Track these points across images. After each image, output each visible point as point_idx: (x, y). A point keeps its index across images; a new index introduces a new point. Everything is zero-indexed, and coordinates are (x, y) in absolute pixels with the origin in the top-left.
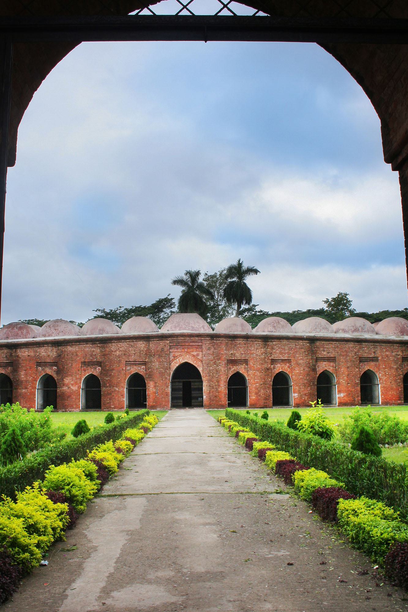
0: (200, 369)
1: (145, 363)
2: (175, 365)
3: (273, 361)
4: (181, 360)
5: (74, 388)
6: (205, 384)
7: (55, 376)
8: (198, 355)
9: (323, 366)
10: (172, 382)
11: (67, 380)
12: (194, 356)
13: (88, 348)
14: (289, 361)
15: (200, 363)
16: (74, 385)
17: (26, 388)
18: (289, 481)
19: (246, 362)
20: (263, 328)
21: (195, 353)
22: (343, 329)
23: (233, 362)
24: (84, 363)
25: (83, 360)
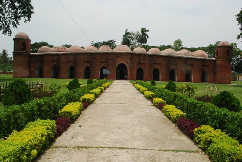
0: (127, 66)
1: (106, 62)
2: (118, 64)
3: (154, 64)
4: (120, 62)
5: (81, 71)
6: (128, 71)
7: (73, 66)
8: (126, 60)
9: (172, 67)
10: (116, 70)
12: (124, 61)
13: (86, 57)
14: (160, 64)
15: (127, 64)
16: (81, 70)
18: (191, 136)
19: (144, 64)
21: (125, 60)
22: (181, 53)
23: (139, 63)
24: (84, 62)
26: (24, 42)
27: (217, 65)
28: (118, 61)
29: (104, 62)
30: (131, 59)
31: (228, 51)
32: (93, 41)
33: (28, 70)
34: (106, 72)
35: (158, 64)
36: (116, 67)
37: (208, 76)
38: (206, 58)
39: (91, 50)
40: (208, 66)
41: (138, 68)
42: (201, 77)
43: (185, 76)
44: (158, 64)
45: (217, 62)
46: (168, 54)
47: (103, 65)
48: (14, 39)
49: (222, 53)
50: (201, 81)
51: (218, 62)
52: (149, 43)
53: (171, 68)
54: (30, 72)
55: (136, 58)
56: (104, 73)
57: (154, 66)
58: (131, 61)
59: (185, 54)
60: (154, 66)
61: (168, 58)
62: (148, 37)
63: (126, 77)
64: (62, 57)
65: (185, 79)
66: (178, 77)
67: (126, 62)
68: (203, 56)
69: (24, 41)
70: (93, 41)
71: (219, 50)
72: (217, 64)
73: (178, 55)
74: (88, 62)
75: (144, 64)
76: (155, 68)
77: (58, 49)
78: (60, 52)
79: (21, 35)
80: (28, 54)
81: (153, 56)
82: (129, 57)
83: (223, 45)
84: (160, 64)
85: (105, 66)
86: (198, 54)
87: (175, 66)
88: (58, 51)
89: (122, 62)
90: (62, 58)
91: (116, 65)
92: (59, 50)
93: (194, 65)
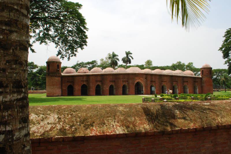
2: (136, 82)
3: (162, 81)
4: (137, 81)
6: (144, 88)
10: (135, 87)
11: (105, 86)
13: (111, 77)
14: (166, 81)
17: (92, 88)
19: (155, 82)
21: (141, 79)
23: (152, 81)
24: (110, 81)
25: (110, 80)
26: (58, 65)
29: (125, 81)
30: (146, 78)
32: (78, 61)
35: (165, 82)
36: (135, 84)
37: (198, 89)
38: (193, 76)
39: (112, 71)
40: (197, 82)
44: (165, 82)
45: (203, 79)
48: (47, 62)
49: (207, 72)
51: (204, 79)
52: (133, 63)
55: (149, 78)
56: (152, 90)
57: (162, 83)
58: (145, 80)
59: (180, 74)
60: (162, 83)
62: (133, 58)
63: (142, 92)
64: (91, 78)
66: (178, 91)
68: (192, 75)
70: (78, 61)
72: (203, 80)
73: (175, 74)
74: (112, 81)
75: (155, 82)
77: (83, 71)
78: (86, 73)
79: (55, 58)
82: (145, 76)
83: (206, 67)
84: (166, 81)
88: (84, 72)
89: (139, 81)
90: (91, 78)
91: (134, 83)
92: (85, 72)
93: (188, 81)
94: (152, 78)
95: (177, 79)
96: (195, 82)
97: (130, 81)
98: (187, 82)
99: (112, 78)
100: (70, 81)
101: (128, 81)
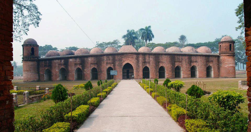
0: (133, 65)
2: (124, 64)
4: (126, 62)
7: (81, 68)
9: (177, 64)
11: (85, 70)
13: (93, 59)
19: (149, 63)
20: (156, 50)
22: (186, 50)
26: (33, 48)
27: (221, 60)
28: (124, 61)
30: (137, 59)
31: (230, 45)
33: (37, 75)
34: (112, 73)
36: (123, 67)
41: (144, 67)
42: (206, 72)
43: (190, 72)
46: (172, 52)
47: (108, 66)
48: (22, 45)
50: (206, 77)
53: (176, 66)
54: (39, 76)
55: (141, 59)
61: (173, 56)
62: (153, 36)
65: (190, 75)
67: (132, 61)
69: (32, 47)
71: (222, 45)
76: (160, 66)
80: (37, 59)
81: (157, 56)
85: (112, 66)
86: (202, 50)
87: (180, 63)
94: (145, 59)
95: (180, 58)
96: (208, 61)
97: (117, 63)
98: (196, 62)
99: (94, 59)
100: (48, 65)
101: (113, 63)
